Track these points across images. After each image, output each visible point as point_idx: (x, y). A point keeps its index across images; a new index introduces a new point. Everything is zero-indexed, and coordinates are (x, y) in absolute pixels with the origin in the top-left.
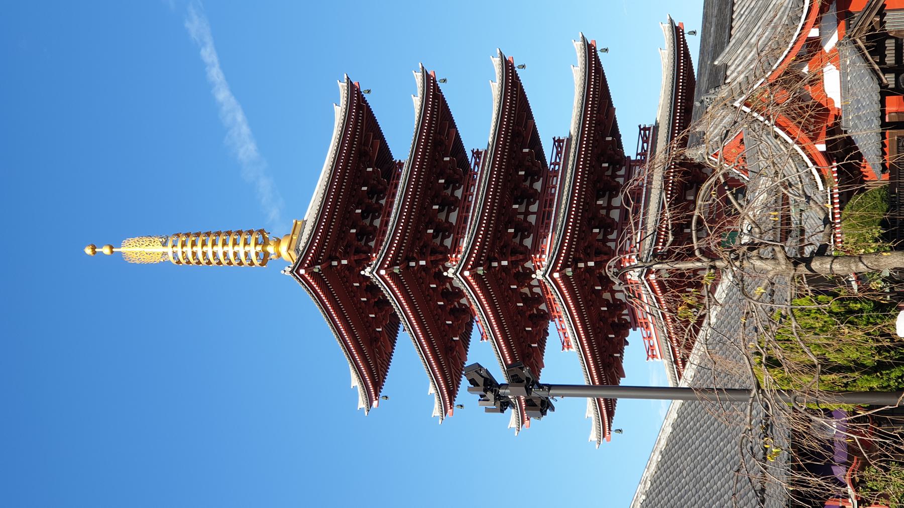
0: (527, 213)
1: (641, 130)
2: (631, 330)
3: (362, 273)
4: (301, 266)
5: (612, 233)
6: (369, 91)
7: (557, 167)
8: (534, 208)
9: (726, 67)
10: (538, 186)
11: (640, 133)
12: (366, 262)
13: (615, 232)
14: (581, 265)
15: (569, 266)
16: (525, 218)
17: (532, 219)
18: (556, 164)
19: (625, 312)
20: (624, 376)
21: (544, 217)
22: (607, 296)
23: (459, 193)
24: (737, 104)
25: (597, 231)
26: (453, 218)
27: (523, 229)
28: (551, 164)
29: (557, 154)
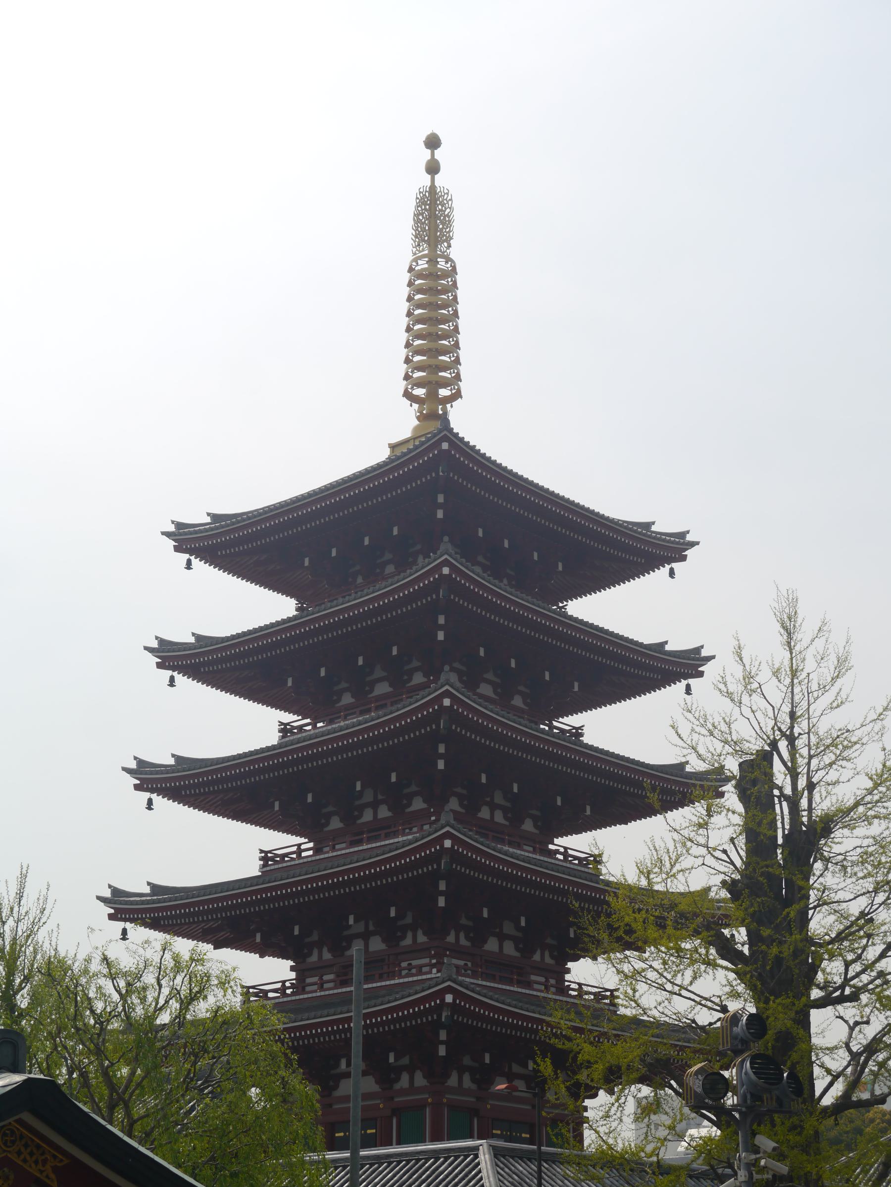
0: (493, 807)
1: (612, 991)
2: (291, 963)
3: (446, 539)
4: (452, 444)
5: (467, 938)
6: (672, 573)
7: (561, 857)
8: (499, 817)
10: (528, 826)
11: (607, 990)
13: (468, 944)
18: (565, 854)
19: (327, 956)
20: (215, 949)
23: (518, 701)
26: (486, 689)
28: (566, 848)
29: (575, 858)
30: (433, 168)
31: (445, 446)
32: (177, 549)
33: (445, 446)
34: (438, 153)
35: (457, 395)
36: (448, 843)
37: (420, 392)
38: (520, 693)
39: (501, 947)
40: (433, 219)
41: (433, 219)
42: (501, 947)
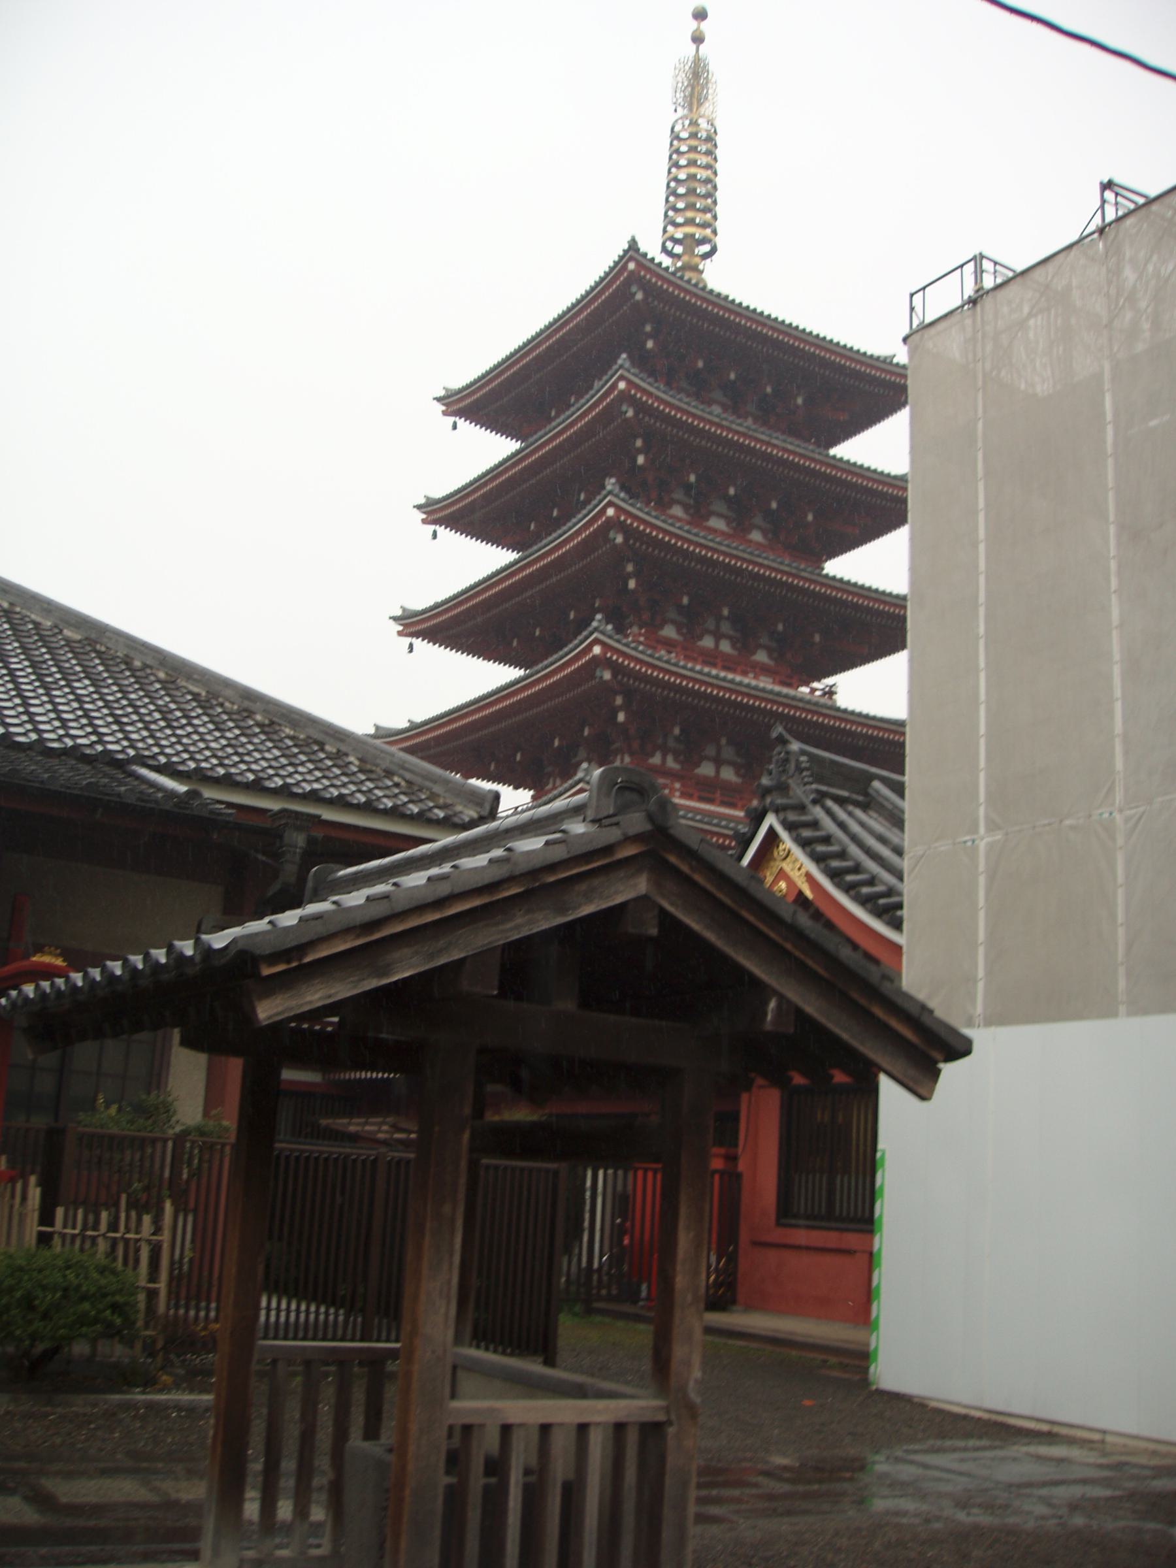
0: (718, 637)
5: (676, 760)
8: (725, 647)
9: (865, 807)
12: (642, 361)
13: (677, 767)
14: (619, 701)
15: (614, 675)
16: (708, 632)
17: (708, 642)
19: (558, 782)
21: (711, 658)
22: (582, 753)
23: (756, 536)
24: (770, 820)
25: (677, 731)
27: (691, 624)
30: (698, 39)
31: (632, 266)
32: (445, 413)
33: (632, 266)
34: (705, 26)
35: (714, 250)
36: (597, 650)
37: (678, 249)
38: (759, 528)
39: (718, 772)
40: (696, 84)
41: (696, 84)
42: (718, 772)
